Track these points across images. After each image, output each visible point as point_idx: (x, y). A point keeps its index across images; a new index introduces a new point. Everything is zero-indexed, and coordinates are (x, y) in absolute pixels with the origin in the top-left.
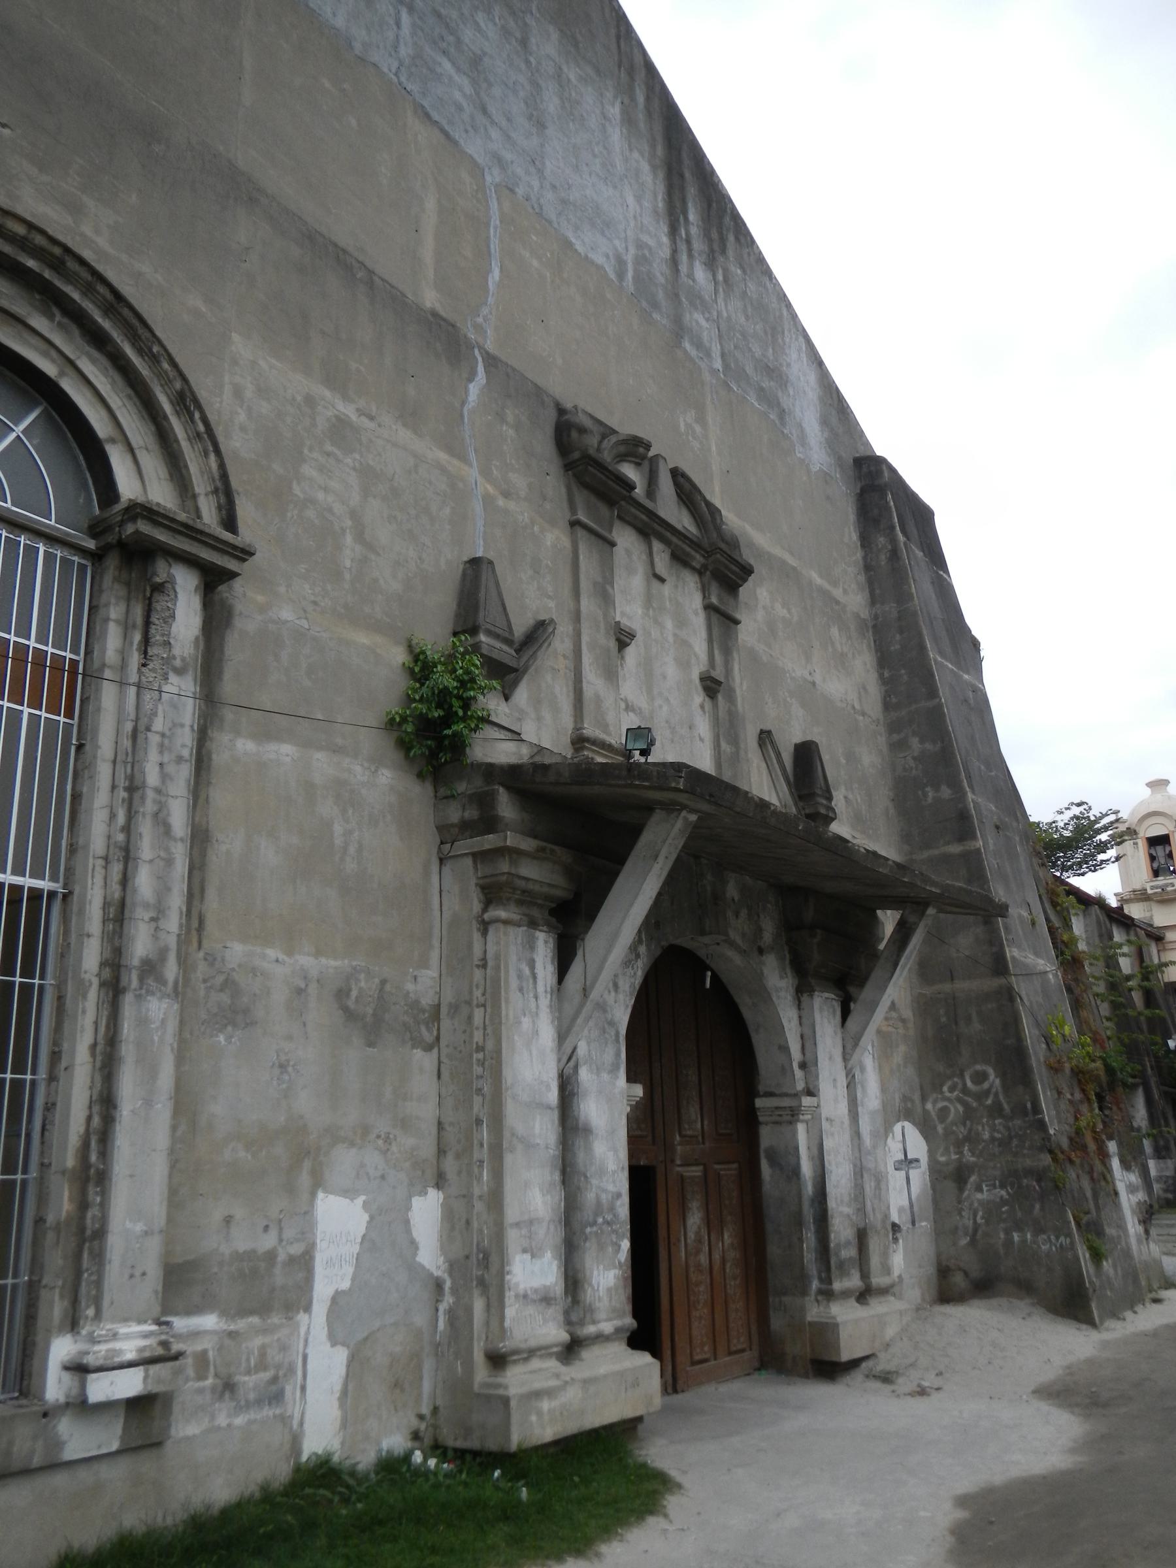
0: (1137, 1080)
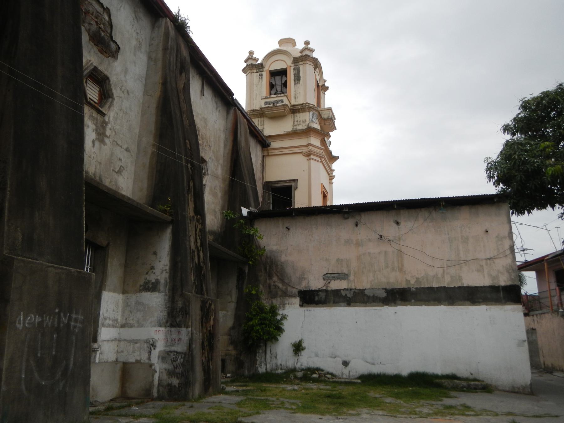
0: (170, 218)
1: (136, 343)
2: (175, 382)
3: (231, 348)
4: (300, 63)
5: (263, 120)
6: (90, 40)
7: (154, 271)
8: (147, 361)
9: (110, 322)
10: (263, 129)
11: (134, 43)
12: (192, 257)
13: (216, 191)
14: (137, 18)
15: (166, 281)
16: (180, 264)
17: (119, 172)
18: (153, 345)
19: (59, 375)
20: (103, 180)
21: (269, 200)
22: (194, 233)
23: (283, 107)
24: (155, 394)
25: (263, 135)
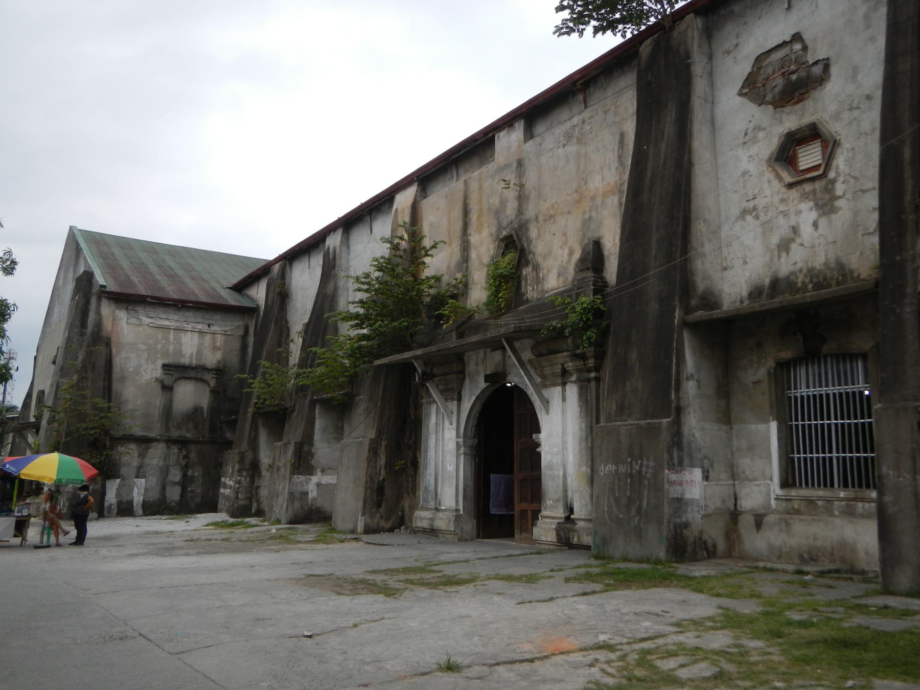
19: (633, 512)
20: (845, 261)
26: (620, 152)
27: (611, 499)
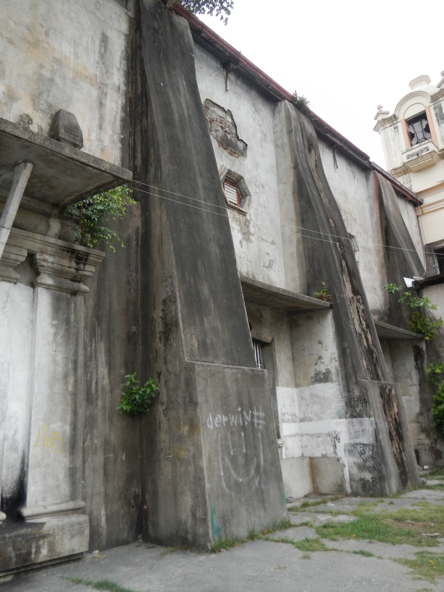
0: (328, 304)
1: (319, 437)
2: (368, 476)
3: (423, 436)
4: (441, 99)
5: (409, 176)
6: (219, 146)
7: (323, 361)
8: (333, 455)
9: (290, 417)
10: (411, 186)
11: (259, 135)
12: (360, 340)
13: (371, 266)
14: (257, 111)
15: (337, 370)
16: (348, 350)
17: (269, 266)
18: (336, 438)
19: (252, 472)
20: (256, 277)
21: (434, 264)
22: (357, 314)
23: (429, 155)
24: (349, 490)
25: (413, 193)
26: (103, 50)
27: (227, 460)
